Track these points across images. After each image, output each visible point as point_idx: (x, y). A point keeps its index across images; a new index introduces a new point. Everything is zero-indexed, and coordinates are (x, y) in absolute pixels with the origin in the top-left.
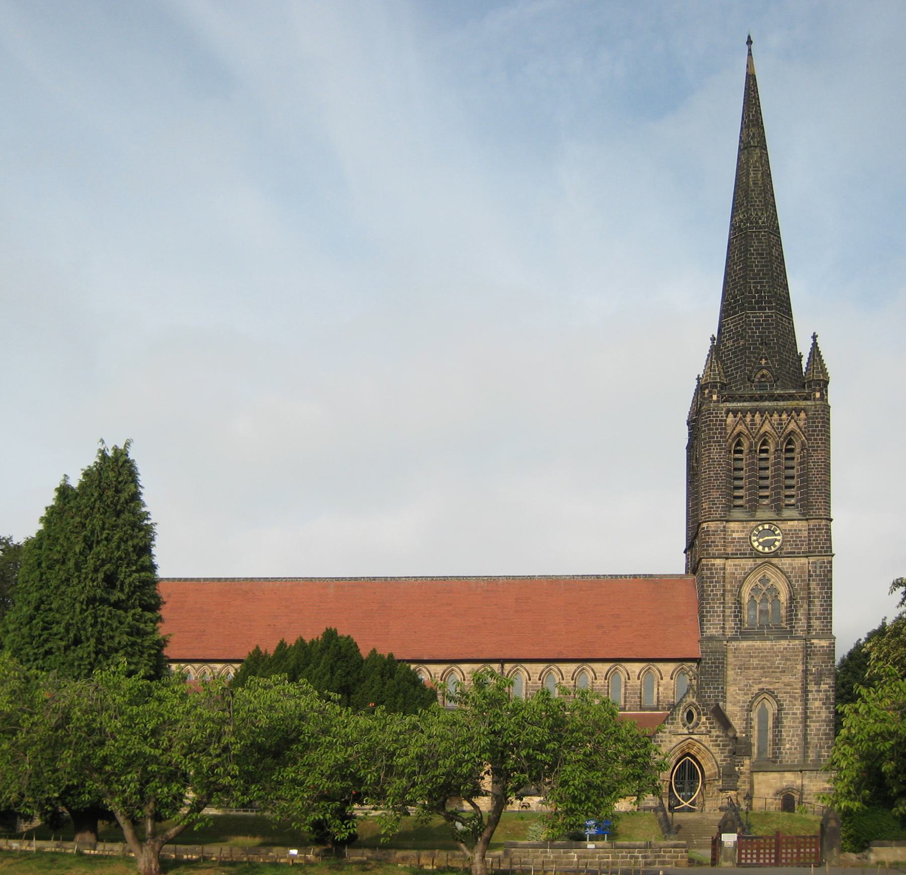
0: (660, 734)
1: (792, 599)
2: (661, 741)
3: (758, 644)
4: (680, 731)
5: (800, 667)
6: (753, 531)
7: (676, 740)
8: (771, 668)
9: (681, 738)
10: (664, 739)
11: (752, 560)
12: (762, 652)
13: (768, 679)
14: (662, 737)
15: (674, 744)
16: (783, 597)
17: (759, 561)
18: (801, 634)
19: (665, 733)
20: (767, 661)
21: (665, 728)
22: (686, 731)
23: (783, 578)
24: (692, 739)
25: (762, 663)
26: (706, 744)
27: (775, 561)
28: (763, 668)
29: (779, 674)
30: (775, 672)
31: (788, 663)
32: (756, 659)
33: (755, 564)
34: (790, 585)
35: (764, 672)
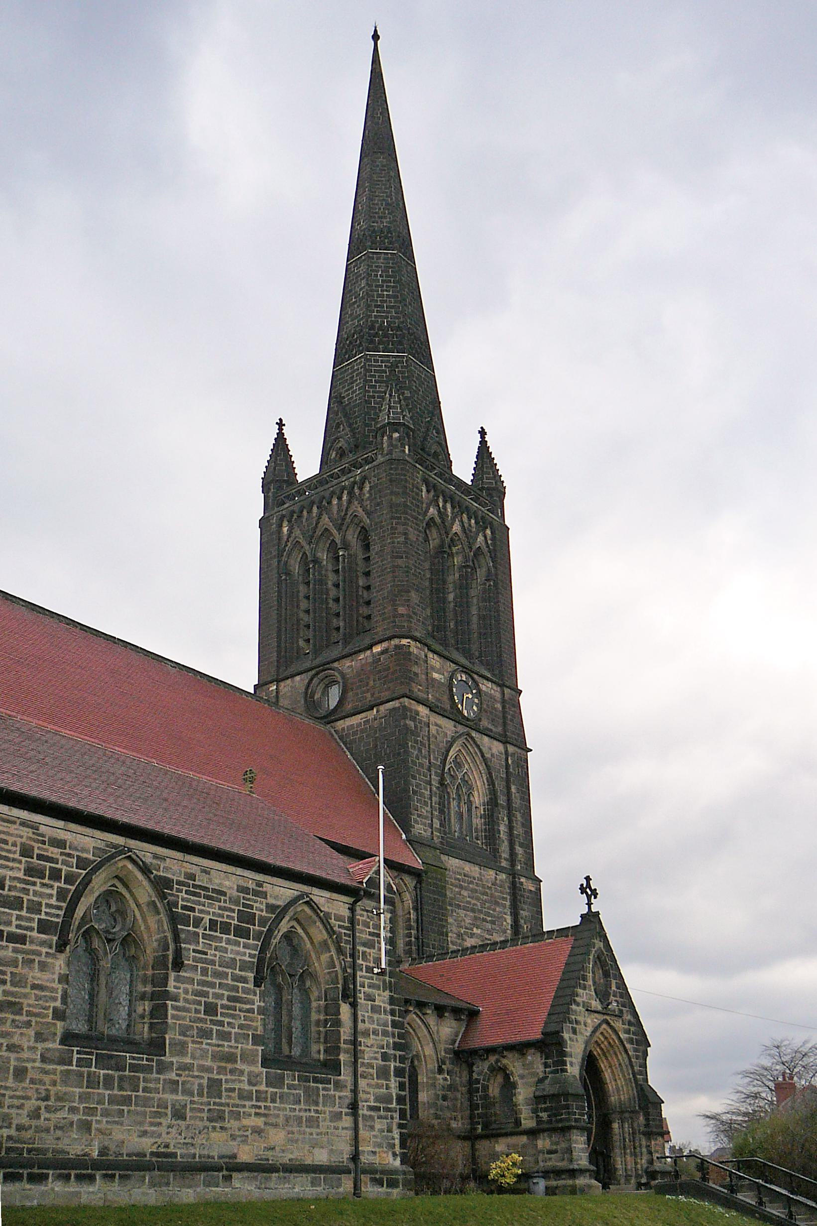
0: (574, 1007)
1: (492, 802)
2: (577, 1022)
3: (468, 867)
5: (509, 919)
6: (451, 678)
8: (480, 911)
10: (579, 1018)
11: (452, 723)
12: (471, 882)
13: (479, 931)
16: (479, 797)
17: (461, 729)
18: (504, 864)
19: (578, 1005)
20: (478, 899)
21: (577, 996)
23: (482, 767)
24: (608, 1023)
25: (473, 902)
26: (623, 1036)
27: (474, 734)
28: (473, 910)
29: (489, 926)
30: (484, 920)
31: (498, 909)
32: (465, 893)
33: (456, 732)
34: (491, 782)
35: (476, 918)
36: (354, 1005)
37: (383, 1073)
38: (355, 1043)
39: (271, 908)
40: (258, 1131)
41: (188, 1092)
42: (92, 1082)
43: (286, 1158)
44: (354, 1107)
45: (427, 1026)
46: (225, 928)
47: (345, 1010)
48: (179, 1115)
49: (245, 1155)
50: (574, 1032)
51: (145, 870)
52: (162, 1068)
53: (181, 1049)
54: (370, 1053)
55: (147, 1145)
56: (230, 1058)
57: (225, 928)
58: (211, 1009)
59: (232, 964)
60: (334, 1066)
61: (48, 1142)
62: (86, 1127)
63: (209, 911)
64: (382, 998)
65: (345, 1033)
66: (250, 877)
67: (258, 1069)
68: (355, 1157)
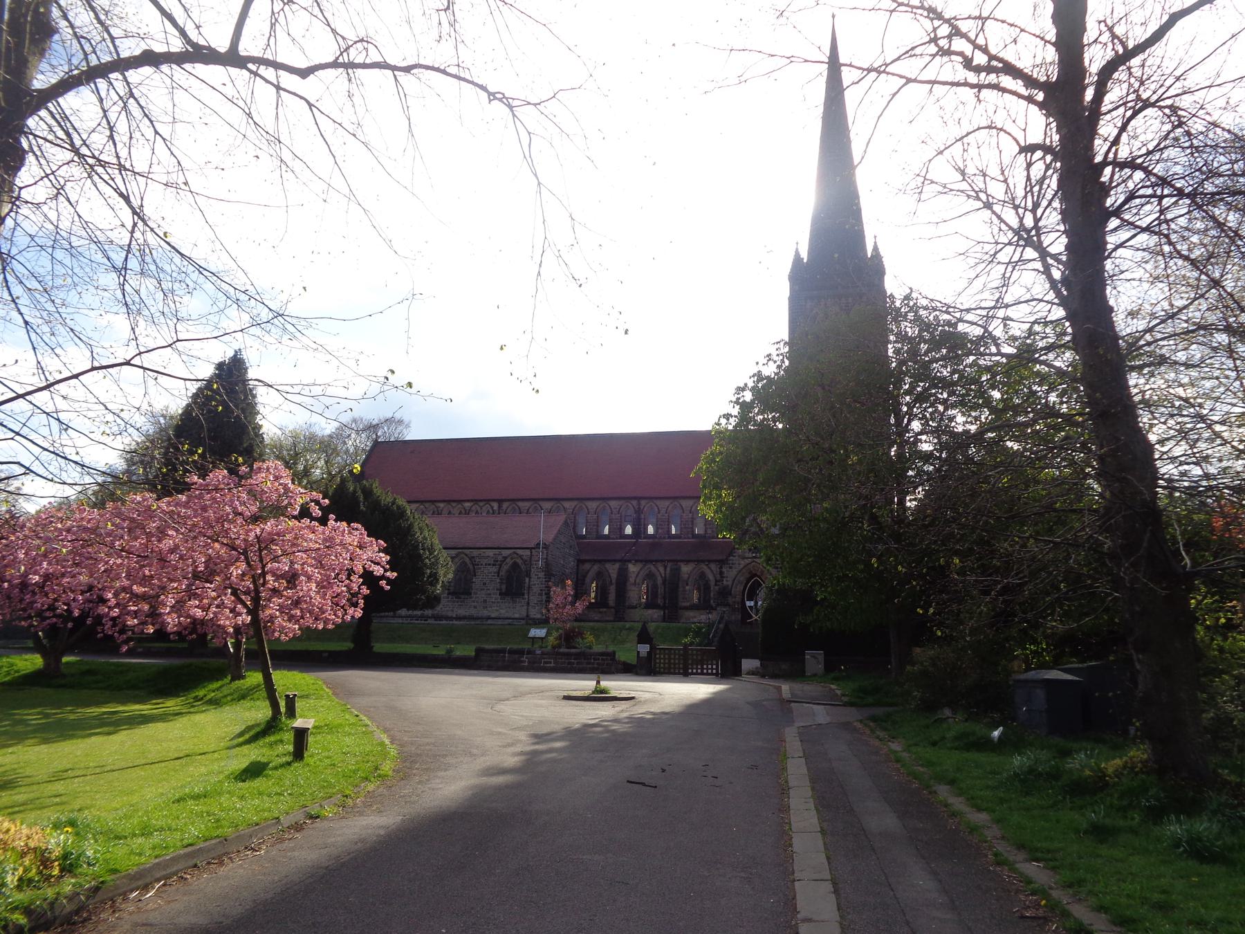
4: (747, 555)
7: (743, 563)
9: (747, 561)
14: (733, 560)
15: (742, 566)
22: (750, 555)
36: (530, 578)
37: (541, 594)
38: (529, 587)
39: (503, 557)
40: (497, 610)
41: (477, 602)
42: (454, 602)
43: (505, 616)
44: (528, 603)
45: (710, 568)
46: (489, 565)
47: (527, 580)
48: (475, 607)
49: (493, 615)
50: (731, 568)
51: (466, 555)
52: (471, 598)
53: (476, 593)
54: (536, 589)
55: (467, 614)
56: (490, 594)
57: (489, 565)
58: (485, 584)
59: (491, 573)
60: (523, 595)
61: (444, 613)
62: (453, 611)
63: (485, 561)
64: (542, 575)
65: (527, 585)
66: (497, 551)
67: (498, 596)
68: (527, 616)
